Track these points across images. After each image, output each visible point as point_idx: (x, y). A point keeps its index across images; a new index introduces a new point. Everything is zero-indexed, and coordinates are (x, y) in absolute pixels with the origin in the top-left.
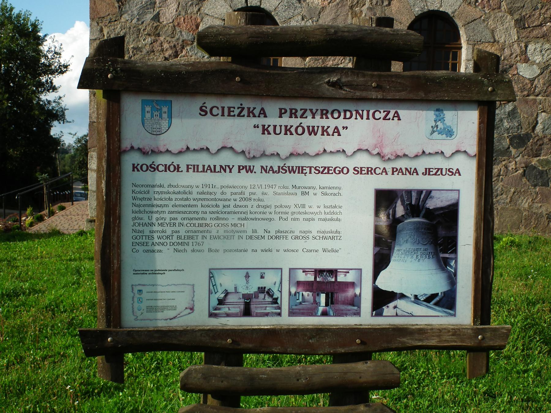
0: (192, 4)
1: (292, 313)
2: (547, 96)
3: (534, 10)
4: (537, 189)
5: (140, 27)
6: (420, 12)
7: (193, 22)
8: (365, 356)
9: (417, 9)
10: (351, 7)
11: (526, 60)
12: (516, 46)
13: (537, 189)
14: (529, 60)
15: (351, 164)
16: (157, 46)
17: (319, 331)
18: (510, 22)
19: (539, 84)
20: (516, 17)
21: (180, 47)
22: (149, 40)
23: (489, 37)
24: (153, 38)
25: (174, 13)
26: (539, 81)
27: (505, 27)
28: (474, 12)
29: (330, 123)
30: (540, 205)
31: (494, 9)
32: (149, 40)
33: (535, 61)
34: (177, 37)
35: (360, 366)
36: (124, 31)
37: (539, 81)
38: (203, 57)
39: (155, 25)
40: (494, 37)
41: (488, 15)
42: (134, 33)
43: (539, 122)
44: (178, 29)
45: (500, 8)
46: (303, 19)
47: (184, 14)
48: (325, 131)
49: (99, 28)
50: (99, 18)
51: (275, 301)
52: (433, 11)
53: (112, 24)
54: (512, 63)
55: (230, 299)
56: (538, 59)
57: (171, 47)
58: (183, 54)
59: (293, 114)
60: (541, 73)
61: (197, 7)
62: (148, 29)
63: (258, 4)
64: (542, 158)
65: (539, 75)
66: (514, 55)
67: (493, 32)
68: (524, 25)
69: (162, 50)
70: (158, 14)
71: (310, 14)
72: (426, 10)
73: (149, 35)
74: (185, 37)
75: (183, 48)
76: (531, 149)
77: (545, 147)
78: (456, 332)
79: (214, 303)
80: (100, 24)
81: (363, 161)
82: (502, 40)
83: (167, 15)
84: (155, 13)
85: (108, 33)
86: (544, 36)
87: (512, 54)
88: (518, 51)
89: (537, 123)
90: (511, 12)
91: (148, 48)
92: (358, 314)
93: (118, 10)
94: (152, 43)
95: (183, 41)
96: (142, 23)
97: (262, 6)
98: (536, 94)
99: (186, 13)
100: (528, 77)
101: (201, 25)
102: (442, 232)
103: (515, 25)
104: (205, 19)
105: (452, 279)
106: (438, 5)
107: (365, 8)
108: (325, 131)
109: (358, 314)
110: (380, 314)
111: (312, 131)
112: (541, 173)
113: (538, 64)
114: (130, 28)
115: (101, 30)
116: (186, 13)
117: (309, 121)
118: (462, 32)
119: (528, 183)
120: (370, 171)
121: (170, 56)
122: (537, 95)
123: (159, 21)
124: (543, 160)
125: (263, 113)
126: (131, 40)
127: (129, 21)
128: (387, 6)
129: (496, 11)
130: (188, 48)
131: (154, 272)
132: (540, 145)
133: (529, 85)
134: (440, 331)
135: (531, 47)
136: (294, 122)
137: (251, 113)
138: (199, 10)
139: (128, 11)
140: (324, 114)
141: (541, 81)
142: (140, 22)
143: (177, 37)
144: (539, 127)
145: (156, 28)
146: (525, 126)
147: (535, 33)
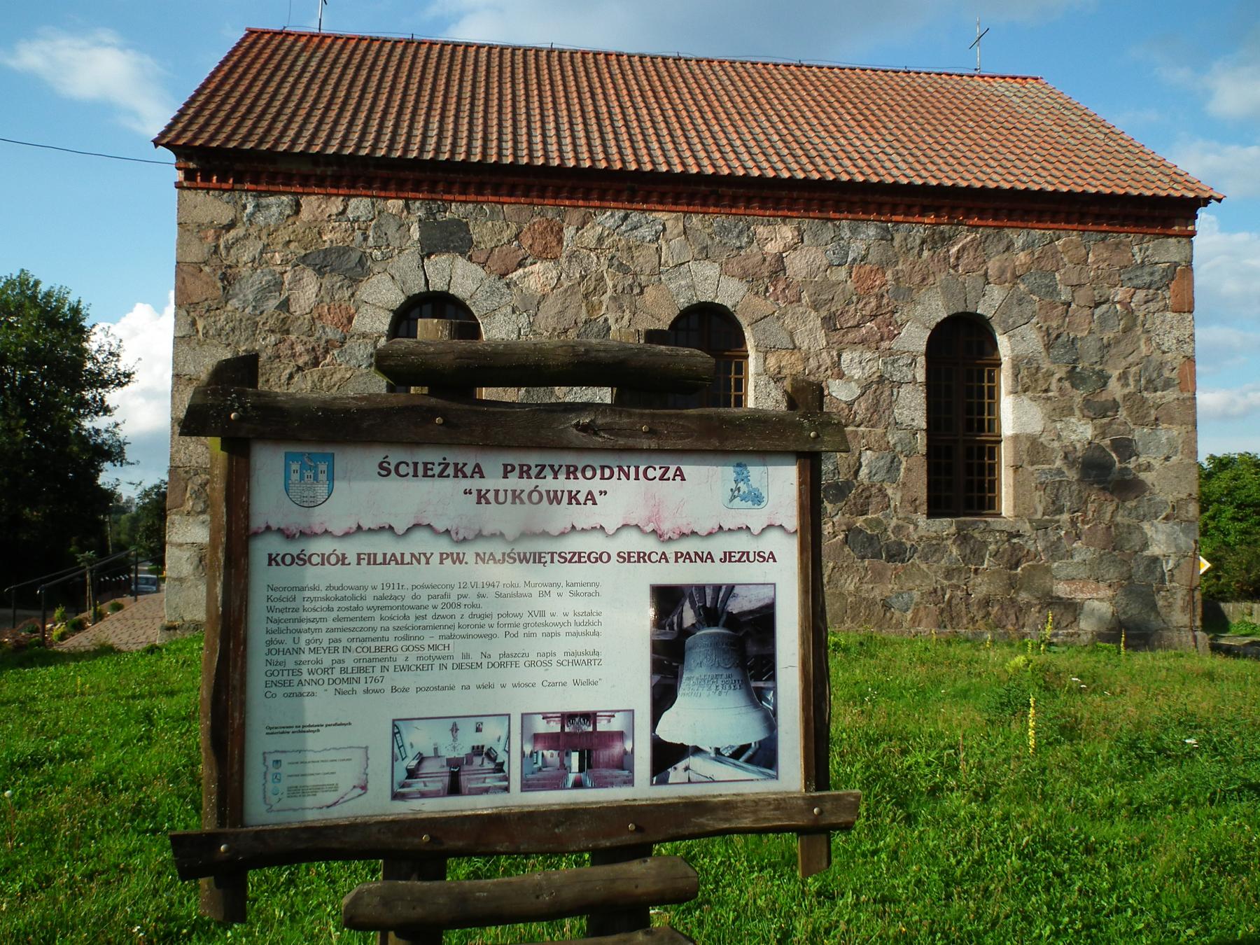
0: (341, 287)
1: (527, 786)
2: (872, 427)
3: (848, 304)
4: (866, 563)
5: (258, 319)
6: (686, 305)
7: (344, 314)
8: (641, 851)
9: (682, 300)
10: (586, 296)
11: (841, 375)
12: (824, 354)
13: (866, 563)
14: (844, 375)
15: (614, 547)
16: (284, 349)
17: (570, 814)
18: (814, 320)
19: (861, 409)
20: (824, 313)
21: (322, 350)
22: (272, 339)
23: (786, 342)
24: (278, 336)
25: (313, 298)
26: (859, 405)
27: (808, 327)
28: (764, 306)
29: (581, 485)
30: (871, 586)
31: (791, 302)
32: (272, 339)
33: (852, 377)
34: (317, 335)
35: (636, 867)
36: (231, 325)
37: (859, 405)
38: (360, 366)
39: (282, 316)
40: (793, 342)
41: (783, 311)
42: (247, 328)
43: (864, 464)
44: (319, 324)
45: (799, 300)
46: (514, 312)
47: (328, 300)
48: (573, 498)
49: (190, 319)
50: (190, 304)
51: (499, 768)
52: (705, 303)
53: (212, 313)
54: (821, 378)
55: (428, 767)
56: (857, 373)
57: (307, 351)
58: (326, 361)
59: (525, 472)
60: (863, 394)
61: (350, 291)
62: (271, 322)
63: (446, 288)
64: (870, 517)
65: (859, 397)
66: (823, 368)
67: (791, 334)
68: (835, 325)
69: (294, 355)
70: (288, 299)
71: (525, 304)
72: (694, 302)
73: (273, 331)
74: (330, 335)
75: (327, 351)
76: (855, 504)
77: (874, 500)
78: (781, 803)
79: (401, 775)
80: (192, 314)
81: (633, 542)
82: (805, 347)
83: (302, 302)
84: (283, 298)
85: (205, 327)
86: (863, 342)
87: (819, 367)
88: (829, 362)
89: (860, 465)
90: (816, 306)
91: (269, 351)
92: (630, 782)
93: (221, 293)
94: (276, 345)
95: (327, 342)
96: (262, 313)
97: (451, 292)
98: (857, 423)
99: (332, 299)
100: (844, 399)
101: (356, 317)
102: (752, 649)
103: (823, 325)
104: (362, 310)
105: (770, 721)
106: (713, 295)
107: (605, 298)
108: (573, 498)
109: (630, 782)
110: (663, 781)
111: (554, 498)
112: (871, 538)
113: (857, 381)
114: (241, 320)
115: (194, 323)
116: (332, 299)
117: (549, 483)
118: (748, 334)
119: (852, 554)
120: (643, 557)
121: (306, 364)
122: (859, 426)
123: (288, 311)
124: (871, 520)
125: (479, 472)
126: (243, 338)
127: (240, 310)
128: (638, 294)
129: (795, 304)
130: (335, 352)
131: (302, 730)
132: (867, 498)
133: (847, 411)
134: (756, 804)
135: (846, 356)
136: (527, 484)
137: (459, 472)
138: (353, 295)
139: (237, 294)
140: (571, 472)
141: (863, 406)
142: (258, 312)
143: (317, 335)
144: (864, 471)
145: (284, 321)
146: (843, 470)
147: (851, 336)
